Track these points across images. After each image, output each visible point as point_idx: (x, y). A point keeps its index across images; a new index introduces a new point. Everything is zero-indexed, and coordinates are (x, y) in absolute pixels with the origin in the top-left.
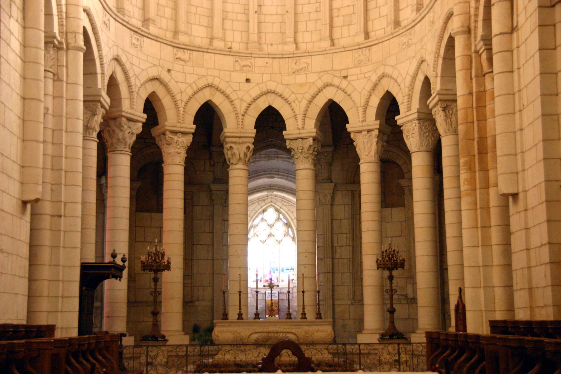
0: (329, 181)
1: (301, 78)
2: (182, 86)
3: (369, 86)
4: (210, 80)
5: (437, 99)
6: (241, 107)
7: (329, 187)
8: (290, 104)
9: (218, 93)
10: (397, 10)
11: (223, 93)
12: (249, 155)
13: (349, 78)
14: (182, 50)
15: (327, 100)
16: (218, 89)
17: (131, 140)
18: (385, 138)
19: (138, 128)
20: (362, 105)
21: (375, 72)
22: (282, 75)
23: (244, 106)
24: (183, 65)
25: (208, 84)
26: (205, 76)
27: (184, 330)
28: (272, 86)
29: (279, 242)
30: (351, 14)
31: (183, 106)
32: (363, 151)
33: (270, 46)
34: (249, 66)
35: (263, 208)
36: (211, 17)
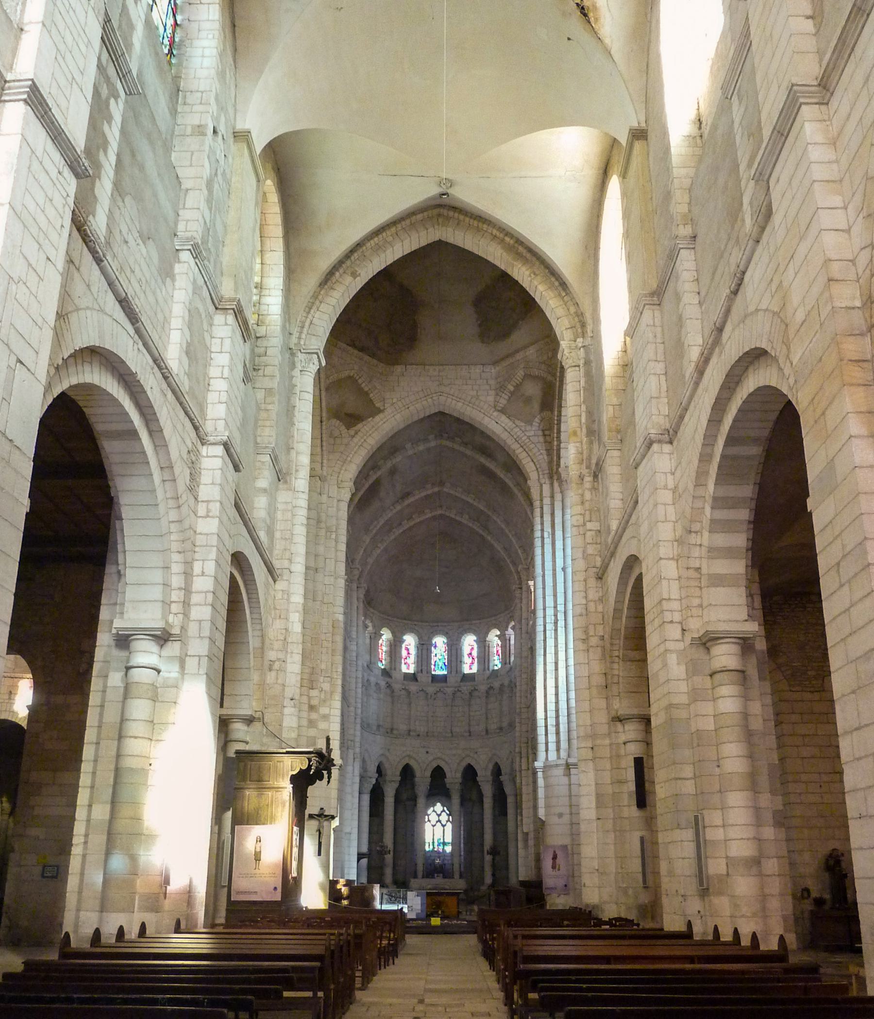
19: (374, 781)
28: (439, 755)
29: (444, 826)
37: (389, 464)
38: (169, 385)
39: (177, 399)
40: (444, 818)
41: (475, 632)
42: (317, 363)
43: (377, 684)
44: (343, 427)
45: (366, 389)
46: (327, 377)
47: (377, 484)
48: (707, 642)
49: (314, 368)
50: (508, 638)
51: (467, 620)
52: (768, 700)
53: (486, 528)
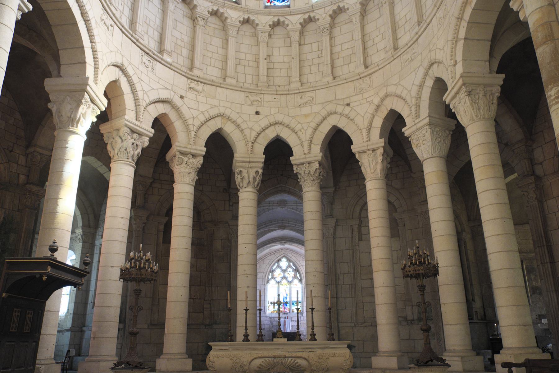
0: (331, 217)
2: (195, 113)
4: (222, 110)
5: (461, 82)
6: (250, 135)
8: (296, 133)
9: (229, 122)
11: (234, 122)
12: (258, 179)
13: (351, 105)
14: (196, 82)
15: (331, 126)
16: (229, 119)
18: (389, 159)
20: (366, 127)
21: (377, 94)
22: (289, 108)
23: (254, 134)
24: (196, 95)
25: (220, 114)
26: (217, 106)
27: (187, 353)
28: (280, 118)
29: (290, 282)
30: (350, 55)
31: (195, 130)
32: (368, 169)
33: (277, 87)
34: (259, 101)
35: (279, 258)
36: (225, 61)
40: (290, 274)
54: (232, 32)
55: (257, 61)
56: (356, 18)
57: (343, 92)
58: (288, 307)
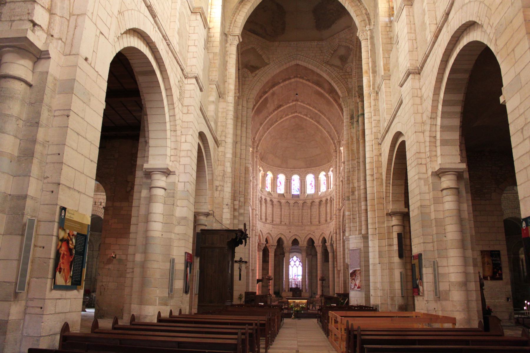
1: (303, 232)
3: (320, 235)
4: (281, 232)
7: (311, 256)
10: (326, 217)
11: (284, 235)
16: (282, 234)
17: (262, 249)
28: (296, 233)
29: (297, 267)
36: (281, 216)
37: (271, 91)
38: (170, 48)
39: (174, 55)
40: (298, 263)
41: (313, 173)
42: (238, 40)
43: (265, 199)
44: (249, 72)
45: (260, 53)
46: (242, 48)
47: (266, 100)
48: (439, 174)
49: (236, 42)
50: (329, 176)
51: (309, 168)
52: (470, 203)
53: (318, 122)
54: (283, 207)
55: (290, 214)
56: (317, 206)
57: (313, 228)
58: (296, 277)
